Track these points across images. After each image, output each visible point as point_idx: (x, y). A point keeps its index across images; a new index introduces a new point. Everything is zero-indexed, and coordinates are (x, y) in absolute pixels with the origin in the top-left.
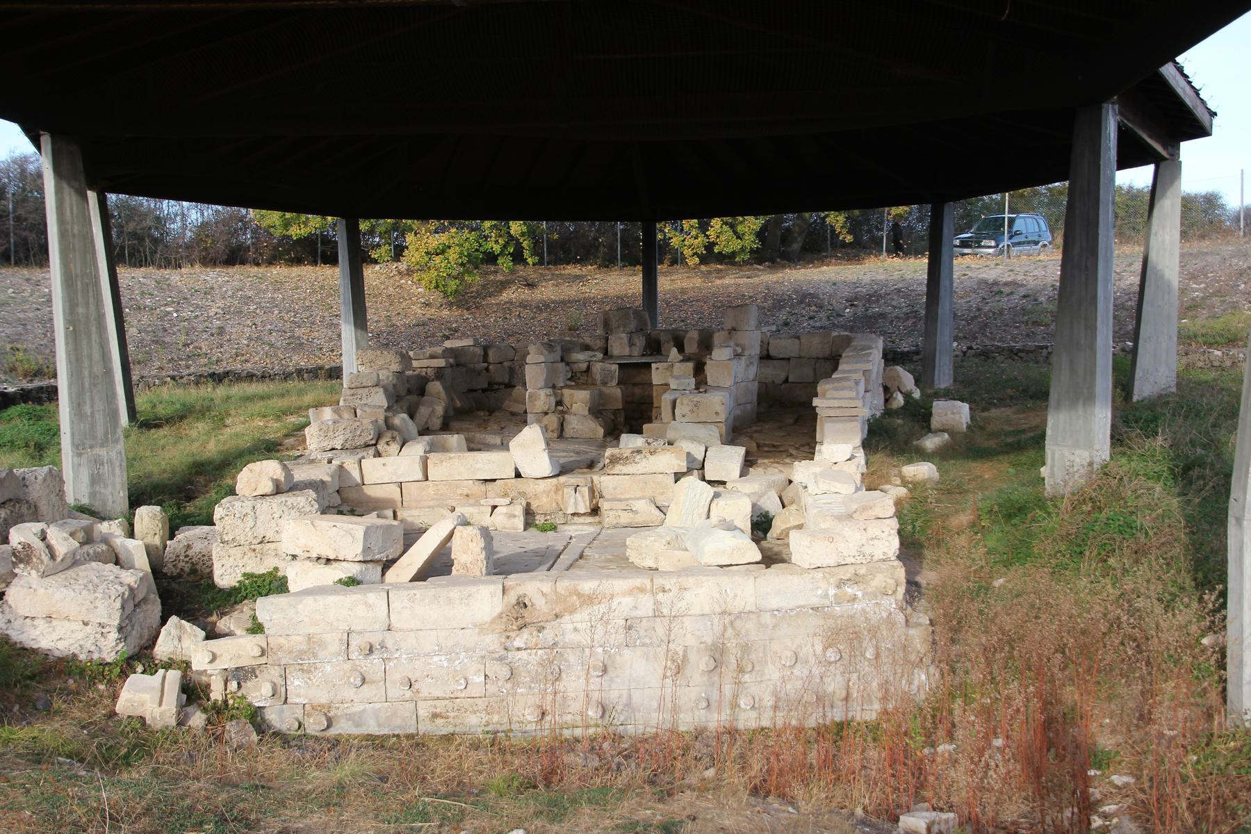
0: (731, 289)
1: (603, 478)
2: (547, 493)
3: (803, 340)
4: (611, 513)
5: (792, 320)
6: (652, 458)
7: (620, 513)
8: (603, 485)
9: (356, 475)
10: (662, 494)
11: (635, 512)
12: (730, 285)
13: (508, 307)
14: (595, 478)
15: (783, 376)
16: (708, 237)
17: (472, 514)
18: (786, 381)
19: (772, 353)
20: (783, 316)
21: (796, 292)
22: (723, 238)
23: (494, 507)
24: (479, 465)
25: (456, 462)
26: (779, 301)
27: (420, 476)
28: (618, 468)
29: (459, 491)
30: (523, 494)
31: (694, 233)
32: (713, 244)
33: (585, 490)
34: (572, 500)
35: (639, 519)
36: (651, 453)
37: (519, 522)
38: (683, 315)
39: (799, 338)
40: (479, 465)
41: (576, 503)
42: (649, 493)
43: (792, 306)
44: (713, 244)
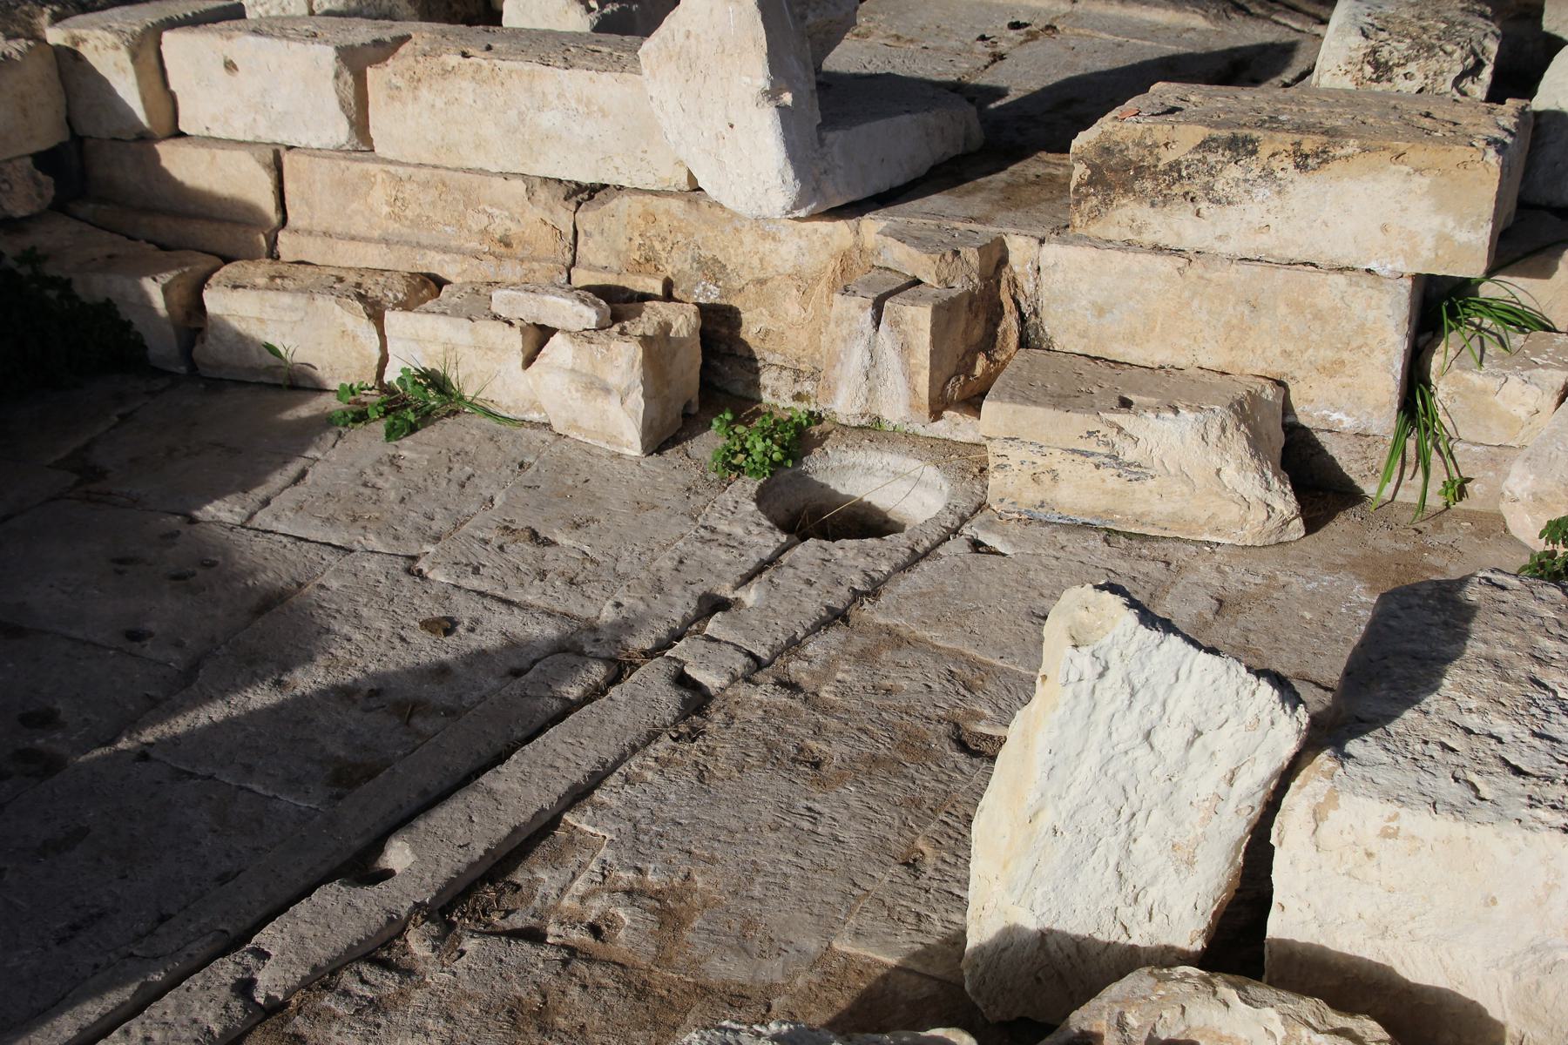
1: (1053, 252)
2: (803, 283)
4: (1015, 455)
6: (1304, 188)
7: (1057, 460)
8: (1052, 283)
9: (127, 88)
10: (1332, 369)
11: (1135, 471)
14: (1020, 248)
17: (449, 347)
23: (541, 335)
24: (549, 119)
25: (464, 88)
27: (339, 131)
28: (1127, 215)
29: (476, 222)
30: (712, 269)
33: (918, 318)
34: (857, 357)
35: (1148, 505)
36: (1302, 162)
37: (619, 422)
40: (549, 119)
41: (871, 372)
42: (1256, 358)
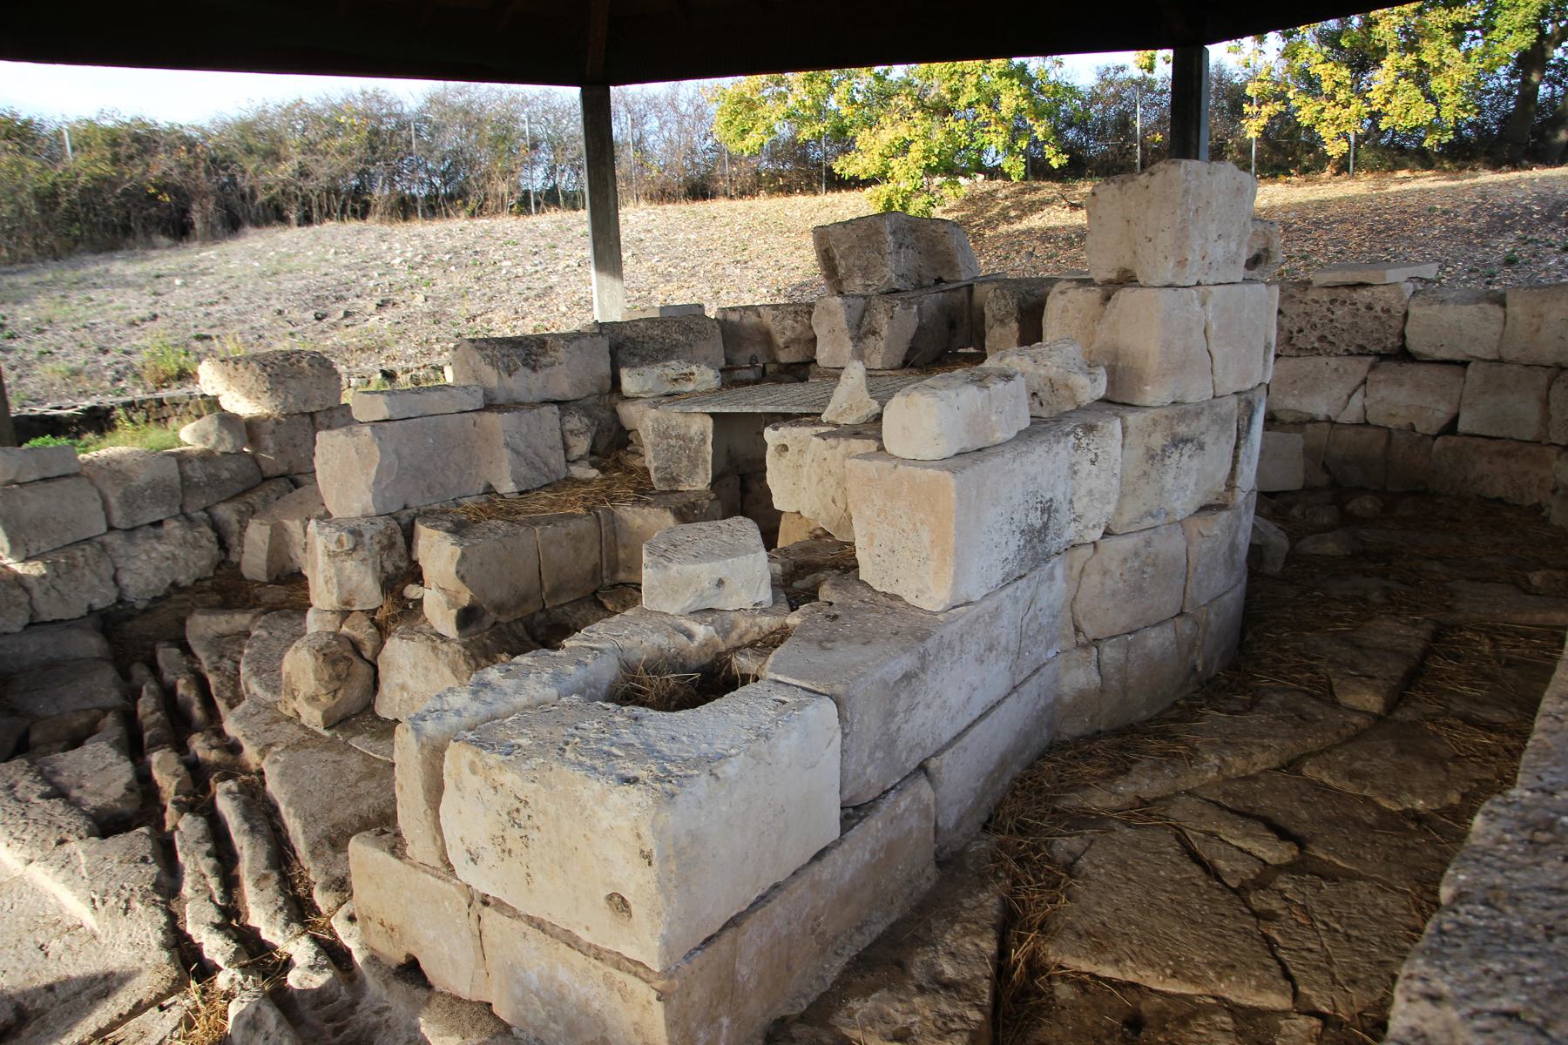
0: (1410, 200)
3: (1516, 308)
5: (1525, 252)
12: (1412, 192)
13: (1013, 241)
15: (1442, 413)
16: (1368, 101)
18: (1451, 427)
19: (1415, 343)
20: (1505, 245)
21: (1541, 199)
22: (1396, 101)
26: (1502, 218)
31: (1341, 96)
32: (1375, 116)
38: (1308, 247)
39: (1500, 301)
43: (1530, 227)
44: (1375, 116)
